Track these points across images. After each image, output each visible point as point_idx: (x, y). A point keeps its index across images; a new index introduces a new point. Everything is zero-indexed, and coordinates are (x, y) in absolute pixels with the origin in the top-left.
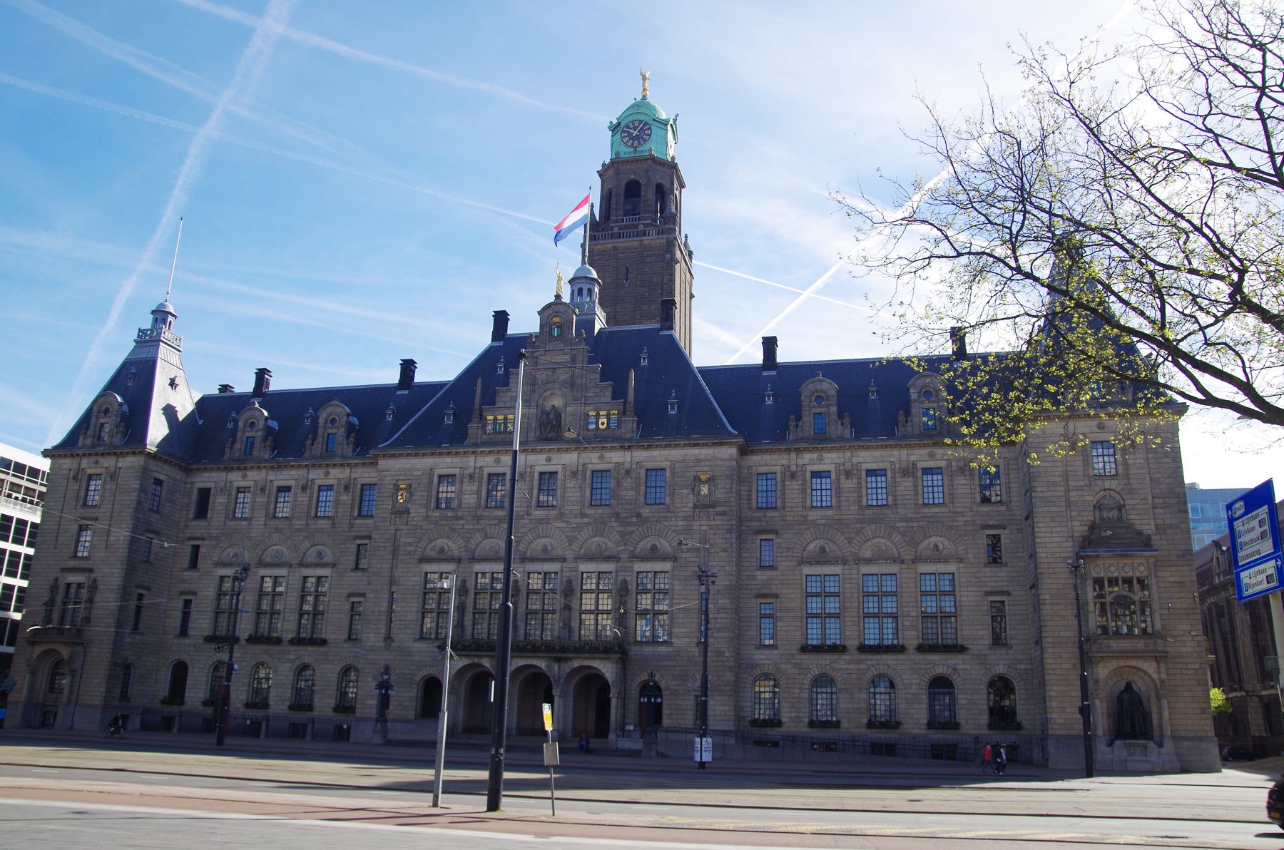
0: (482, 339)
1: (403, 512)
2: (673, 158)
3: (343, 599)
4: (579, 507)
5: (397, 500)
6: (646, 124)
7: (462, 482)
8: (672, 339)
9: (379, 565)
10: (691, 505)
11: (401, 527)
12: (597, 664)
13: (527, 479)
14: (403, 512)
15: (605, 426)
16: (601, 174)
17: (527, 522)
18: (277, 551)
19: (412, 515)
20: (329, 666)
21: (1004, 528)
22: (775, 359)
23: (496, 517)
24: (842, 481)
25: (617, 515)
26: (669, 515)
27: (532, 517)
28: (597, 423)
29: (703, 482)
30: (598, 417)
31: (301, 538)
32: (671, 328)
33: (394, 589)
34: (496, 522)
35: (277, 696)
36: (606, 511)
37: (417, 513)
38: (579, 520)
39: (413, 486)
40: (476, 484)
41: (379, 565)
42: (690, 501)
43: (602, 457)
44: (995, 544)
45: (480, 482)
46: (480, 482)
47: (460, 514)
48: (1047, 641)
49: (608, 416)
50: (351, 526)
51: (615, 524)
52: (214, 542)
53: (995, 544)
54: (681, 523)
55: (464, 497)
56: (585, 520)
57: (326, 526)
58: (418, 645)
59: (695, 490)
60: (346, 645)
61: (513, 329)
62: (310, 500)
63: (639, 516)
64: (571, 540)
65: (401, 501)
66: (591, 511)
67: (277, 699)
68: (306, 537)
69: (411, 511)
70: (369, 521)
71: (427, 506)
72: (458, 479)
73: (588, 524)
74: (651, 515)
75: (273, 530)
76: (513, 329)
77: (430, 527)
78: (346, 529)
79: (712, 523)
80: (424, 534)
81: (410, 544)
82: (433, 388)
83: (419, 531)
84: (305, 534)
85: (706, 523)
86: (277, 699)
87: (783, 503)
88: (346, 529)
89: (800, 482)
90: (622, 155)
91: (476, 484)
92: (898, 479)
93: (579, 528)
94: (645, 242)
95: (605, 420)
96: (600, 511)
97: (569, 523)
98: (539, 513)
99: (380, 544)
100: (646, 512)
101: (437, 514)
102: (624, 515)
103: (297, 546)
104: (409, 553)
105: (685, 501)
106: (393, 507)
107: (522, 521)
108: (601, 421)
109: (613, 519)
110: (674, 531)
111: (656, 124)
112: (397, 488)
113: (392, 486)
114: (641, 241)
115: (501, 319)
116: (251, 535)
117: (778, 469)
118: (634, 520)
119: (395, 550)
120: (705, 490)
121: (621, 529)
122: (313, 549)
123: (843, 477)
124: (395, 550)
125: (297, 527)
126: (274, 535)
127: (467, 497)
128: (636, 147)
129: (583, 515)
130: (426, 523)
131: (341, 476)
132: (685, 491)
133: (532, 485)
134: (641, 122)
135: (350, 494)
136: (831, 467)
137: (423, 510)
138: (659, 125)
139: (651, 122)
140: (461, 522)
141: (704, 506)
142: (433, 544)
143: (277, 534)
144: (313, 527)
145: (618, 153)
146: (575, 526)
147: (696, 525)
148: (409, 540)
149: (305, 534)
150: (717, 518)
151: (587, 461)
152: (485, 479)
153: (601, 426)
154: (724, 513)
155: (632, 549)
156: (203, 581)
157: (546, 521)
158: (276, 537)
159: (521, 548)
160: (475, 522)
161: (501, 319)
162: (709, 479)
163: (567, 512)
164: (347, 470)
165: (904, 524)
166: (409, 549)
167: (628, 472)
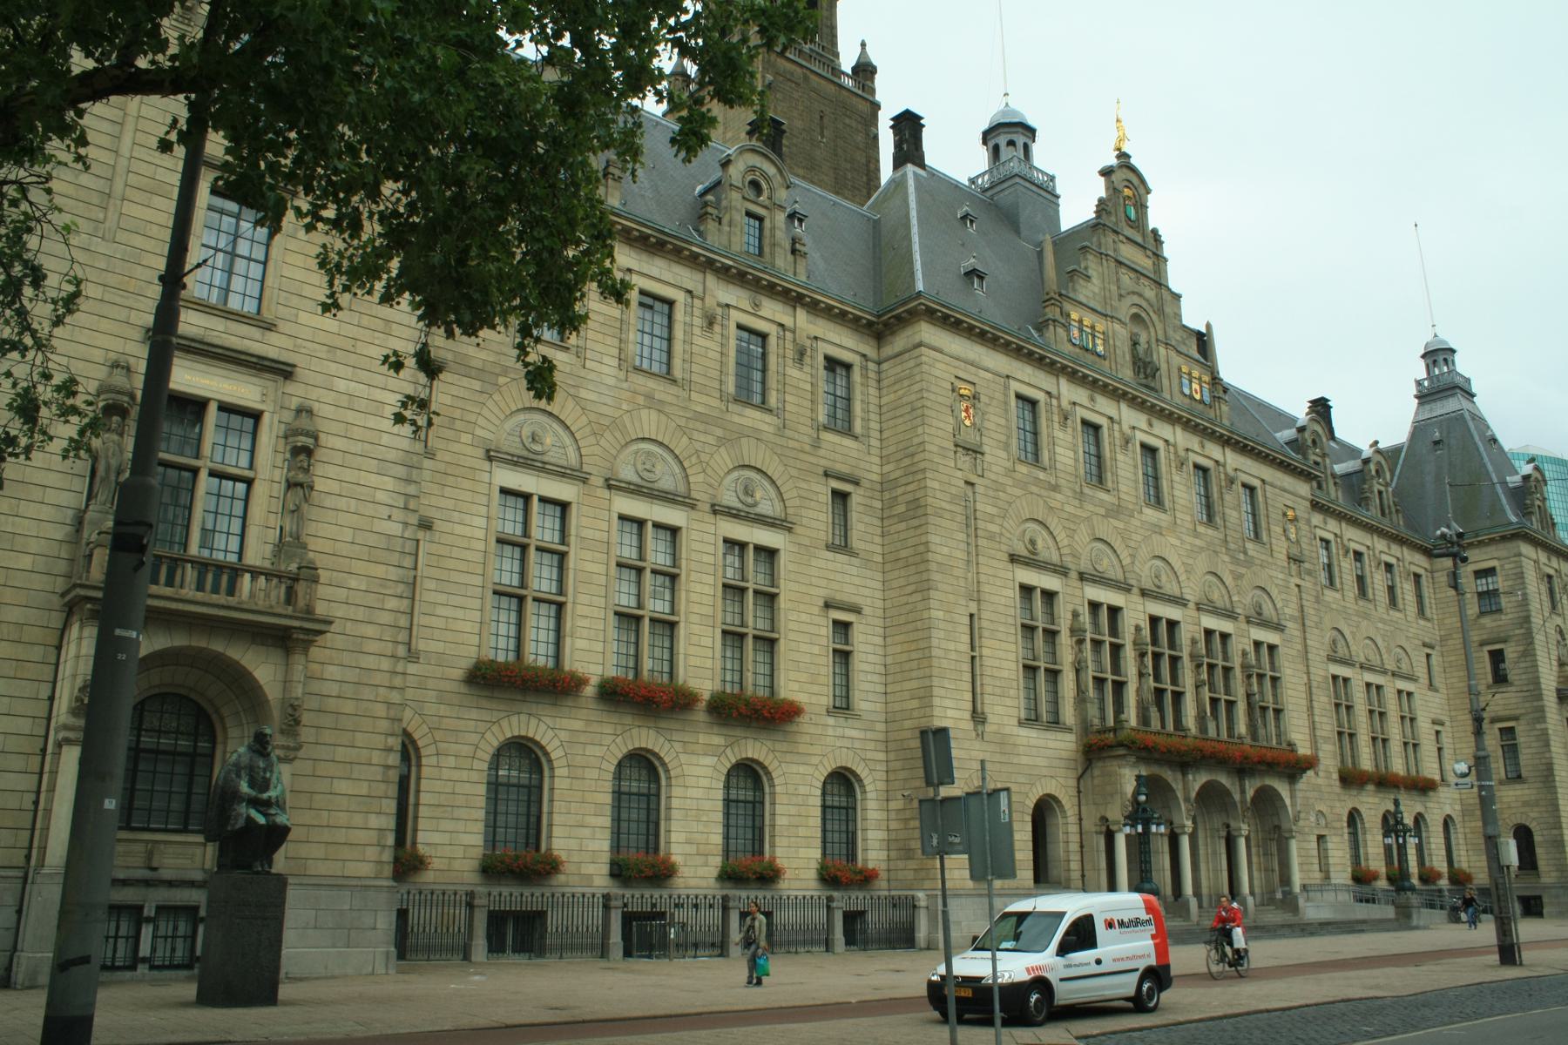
3: (816, 610)
9: (945, 551)
18: (649, 454)
19: (987, 458)
20: (802, 769)
23: (1102, 503)
31: (710, 439)
34: (1102, 511)
35: (688, 842)
41: (945, 551)
50: (816, 444)
52: (477, 385)
57: (766, 428)
58: (1024, 732)
60: (831, 721)
67: (692, 849)
68: (722, 442)
70: (848, 442)
75: (641, 400)
78: (807, 448)
81: (991, 518)
84: (719, 432)
86: (692, 849)
88: (807, 448)
97: (1183, 542)
99: (944, 505)
103: (704, 457)
104: (991, 537)
116: (583, 394)
122: (735, 474)
125: (699, 409)
126: (644, 413)
130: (1010, 482)
131: (787, 321)
135: (807, 369)
143: (654, 415)
144: (736, 419)
149: (719, 432)
156: (448, 491)
157: (1157, 529)
160: (1077, 503)
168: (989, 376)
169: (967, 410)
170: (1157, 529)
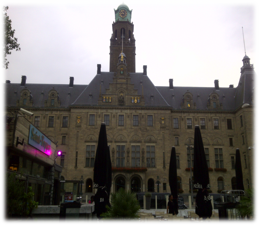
0: (95, 73)
1: (79, 126)
2: (132, 23)
4: (130, 126)
5: (77, 122)
6: (126, 11)
7: (97, 117)
10: (160, 126)
11: (79, 131)
13: (116, 117)
17: (116, 130)
19: (82, 127)
21: (233, 136)
22: (173, 86)
24: (195, 121)
25: (140, 129)
26: (154, 129)
27: (118, 129)
29: (162, 120)
32: (146, 74)
36: (138, 127)
37: (84, 126)
39: (82, 117)
40: (101, 118)
44: (231, 140)
45: (102, 117)
46: (102, 117)
47: (96, 127)
51: (140, 131)
53: (231, 140)
54: (157, 132)
55: (98, 122)
56: (132, 130)
59: (161, 123)
62: (46, 121)
63: (146, 129)
64: (128, 136)
65: (79, 122)
66: (133, 127)
69: (82, 126)
71: (86, 124)
72: (95, 116)
74: (150, 129)
77: (88, 131)
79: (165, 132)
80: (86, 133)
82: (81, 88)
83: (84, 132)
85: (163, 132)
87: (180, 127)
89: (184, 121)
90: (120, 20)
91: (101, 118)
92: (208, 122)
96: (136, 127)
98: (119, 127)
100: (148, 128)
101: (90, 127)
102: (142, 129)
105: (158, 126)
106: (76, 124)
107: (115, 130)
109: (140, 130)
110: (156, 134)
112: (77, 118)
113: (75, 117)
115: (99, 66)
117: (178, 117)
118: (145, 130)
119: (77, 138)
120: (163, 122)
121: (141, 133)
123: (195, 120)
124: (77, 138)
127: (99, 122)
128: (123, 18)
129: (132, 128)
131: (56, 113)
132: (158, 122)
133: (117, 119)
134: (124, 10)
136: (192, 117)
137: (85, 125)
139: (127, 11)
140: (97, 129)
141: (163, 127)
142: (89, 136)
145: (118, 19)
146: (129, 131)
147: (161, 133)
148: (81, 135)
150: (167, 130)
152: (103, 116)
154: (168, 129)
155: (145, 139)
157: (121, 130)
159: (114, 138)
161: (99, 66)
162: (164, 119)
163: (127, 127)
164: (59, 112)
166: (81, 138)
167: (143, 116)
168: (84, 113)
169: (79, 120)
170: (121, 130)
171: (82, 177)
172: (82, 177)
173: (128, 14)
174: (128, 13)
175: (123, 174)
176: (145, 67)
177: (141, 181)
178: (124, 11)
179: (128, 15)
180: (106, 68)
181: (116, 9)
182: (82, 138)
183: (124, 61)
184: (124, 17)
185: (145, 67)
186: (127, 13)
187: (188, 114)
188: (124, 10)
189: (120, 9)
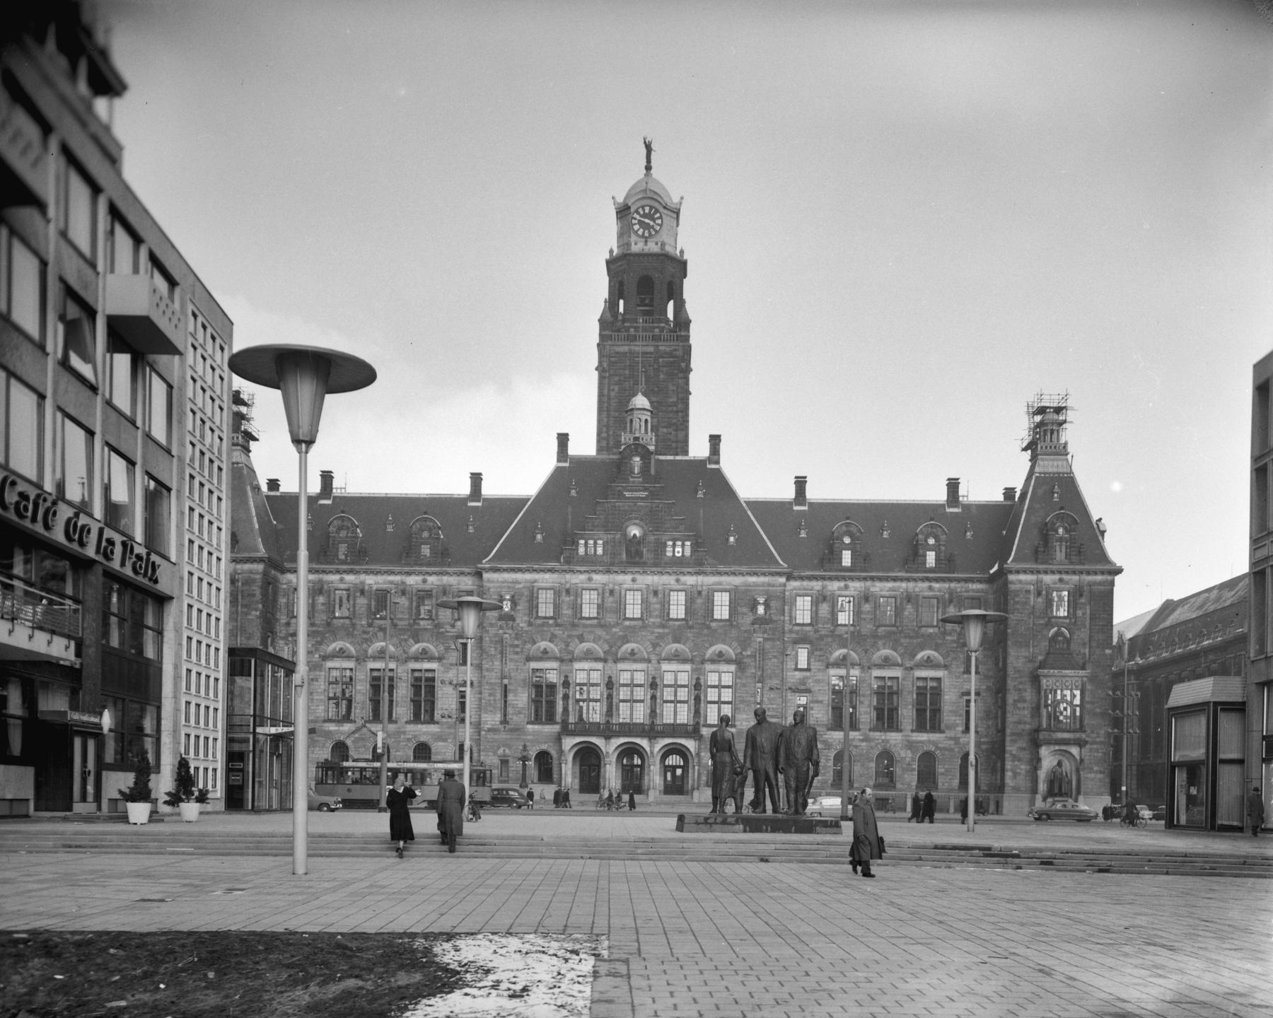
2: (682, 252)
6: (657, 211)
8: (719, 472)
12: (638, 740)
14: (510, 618)
15: (680, 555)
16: (608, 263)
28: (674, 551)
30: (674, 546)
32: (718, 462)
33: (506, 681)
38: (660, 630)
42: (749, 619)
43: (678, 581)
48: (1008, 731)
49: (683, 546)
61: (574, 449)
73: (668, 634)
76: (574, 449)
82: (510, 506)
93: (661, 637)
94: (661, 348)
95: (680, 550)
108: (677, 550)
111: (666, 211)
114: (657, 346)
115: (563, 439)
134: (651, 208)
138: (669, 213)
139: (661, 210)
151: (667, 582)
153: (677, 555)
158: (380, 635)
161: (563, 439)
165: (908, 640)
171: (525, 746)
172: (525, 746)
173: (668, 220)
174: (664, 216)
175: (638, 740)
176: (715, 440)
177: (690, 758)
178: (650, 210)
179: (664, 225)
180: (585, 445)
181: (620, 199)
182: (518, 650)
183: (646, 421)
184: (650, 232)
185: (715, 440)
186: (661, 217)
187: (842, 584)
188: (651, 208)
189: (639, 204)
